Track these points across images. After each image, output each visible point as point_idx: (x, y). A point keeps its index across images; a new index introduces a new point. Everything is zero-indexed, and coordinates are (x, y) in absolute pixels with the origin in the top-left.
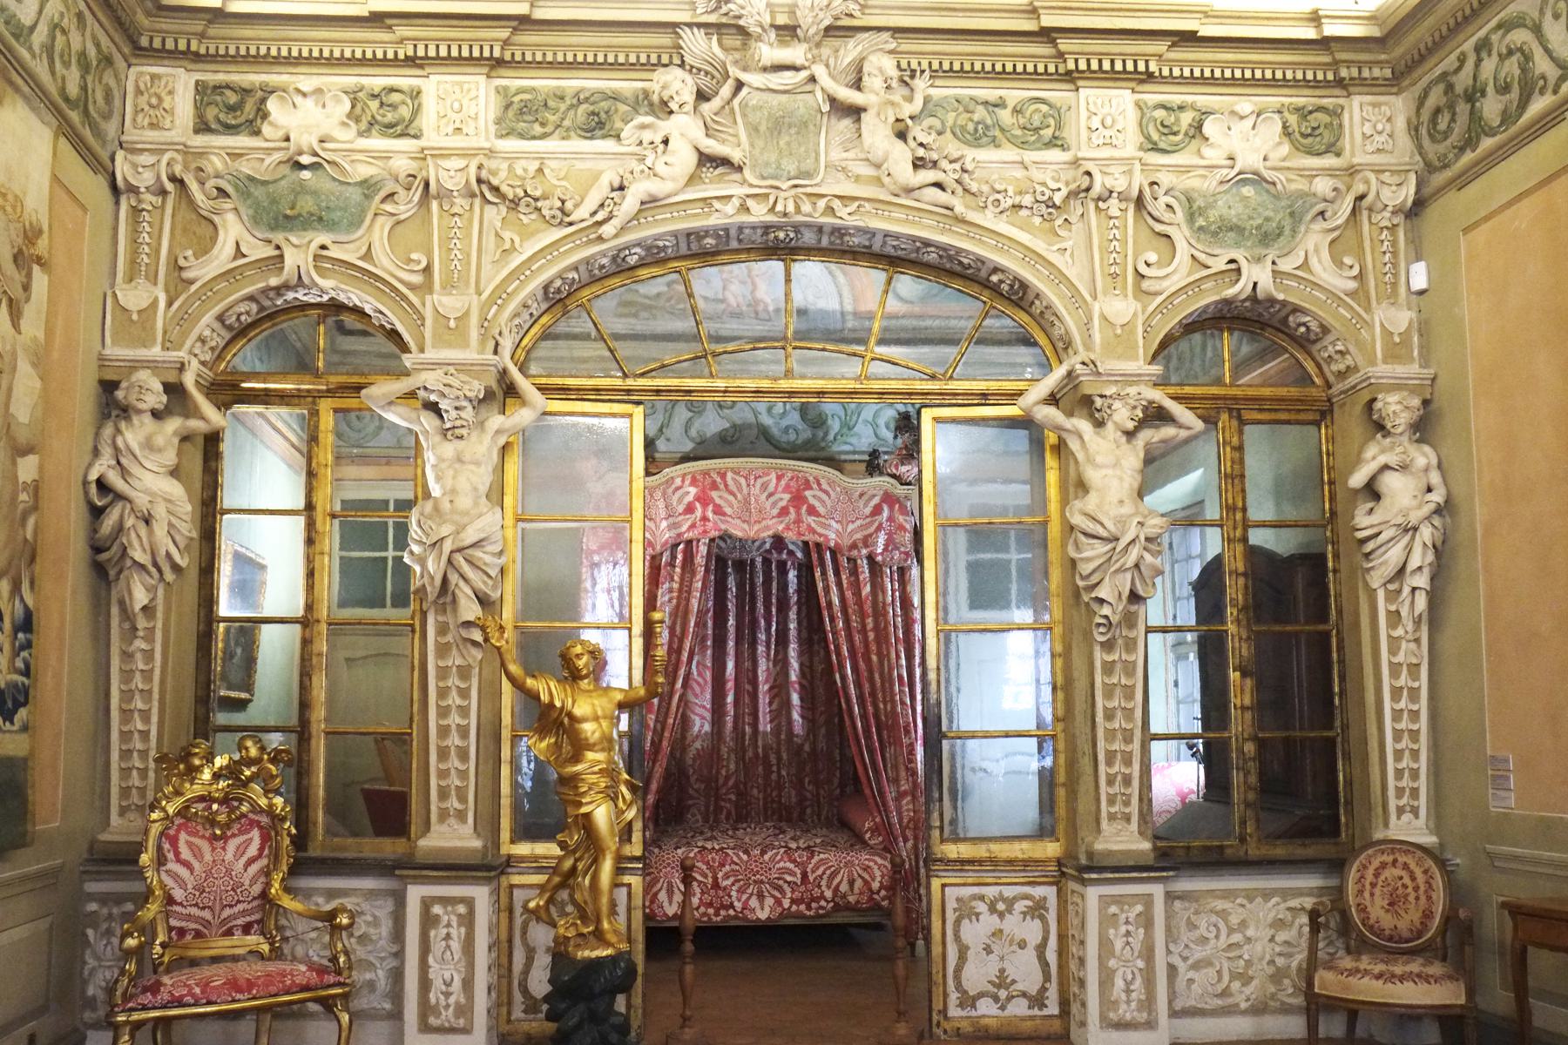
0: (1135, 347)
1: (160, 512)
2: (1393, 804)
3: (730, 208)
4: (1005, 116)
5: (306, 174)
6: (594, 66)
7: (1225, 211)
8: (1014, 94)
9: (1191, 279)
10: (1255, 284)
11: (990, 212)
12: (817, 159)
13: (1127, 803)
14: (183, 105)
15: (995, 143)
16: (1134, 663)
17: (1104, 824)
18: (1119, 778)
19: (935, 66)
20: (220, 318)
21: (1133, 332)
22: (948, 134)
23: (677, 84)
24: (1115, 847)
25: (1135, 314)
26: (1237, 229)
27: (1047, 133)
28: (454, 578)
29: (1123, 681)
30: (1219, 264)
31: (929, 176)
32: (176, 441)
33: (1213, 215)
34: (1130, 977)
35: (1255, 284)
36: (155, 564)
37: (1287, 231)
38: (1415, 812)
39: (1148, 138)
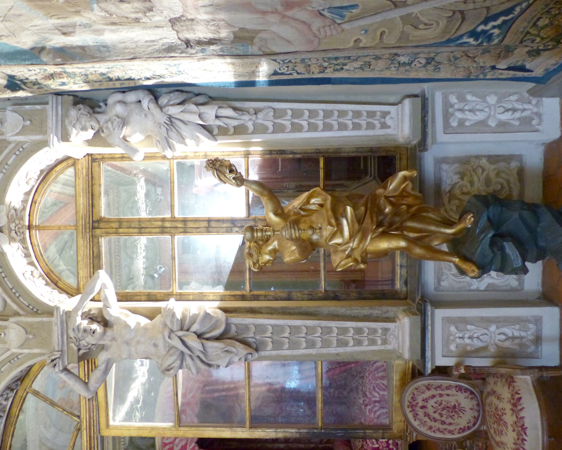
0: (43, 323)
2: (378, 132)
13: (375, 331)
16: (273, 326)
17: (389, 347)
18: (356, 337)
21: (31, 325)
24: (407, 343)
25: (17, 323)
29: (286, 335)
34: (503, 337)
38: (385, 114)
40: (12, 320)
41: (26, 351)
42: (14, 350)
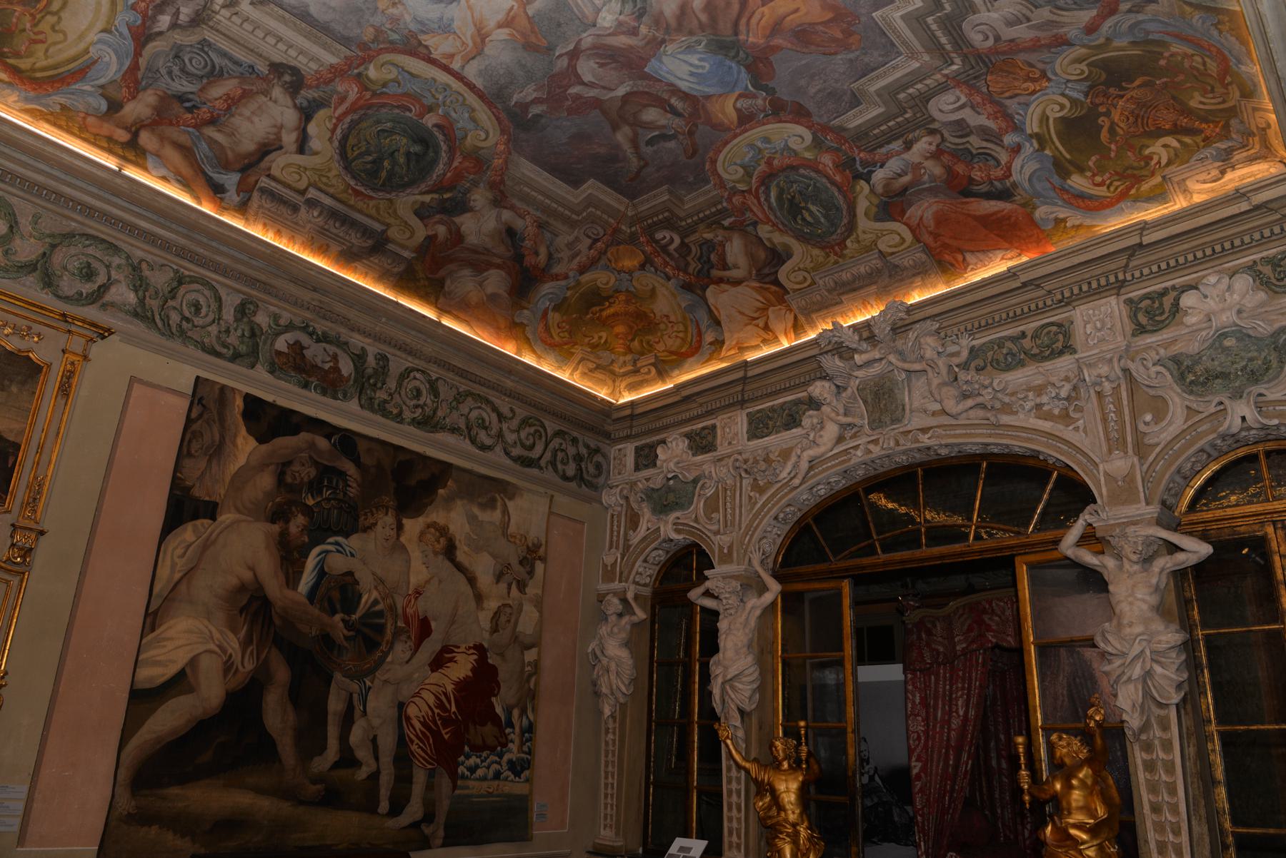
1: (613, 666)
3: (859, 453)
4: (1027, 343)
5: (671, 482)
6: (786, 389)
7: (1209, 364)
8: (1031, 326)
9: (1190, 423)
10: (1243, 418)
11: (1021, 416)
12: (904, 409)
14: (630, 460)
15: (1021, 364)
19: (969, 327)
20: (645, 561)
21: (1133, 480)
22: (989, 368)
23: (820, 389)
25: (1133, 466)
26: (1224, 375)
27: (1059, 345)
28: (726, 698)
30: (1212, 409)
31: (970, 403)
32: (628, 627)
33: (1199, 369)
35: (1243, 418)
36: (612, 694)
37: (1275, 364)
39: (1139, 324)
40: (1136, 459)
41: (1102, 479)
42: (1101, 467)
